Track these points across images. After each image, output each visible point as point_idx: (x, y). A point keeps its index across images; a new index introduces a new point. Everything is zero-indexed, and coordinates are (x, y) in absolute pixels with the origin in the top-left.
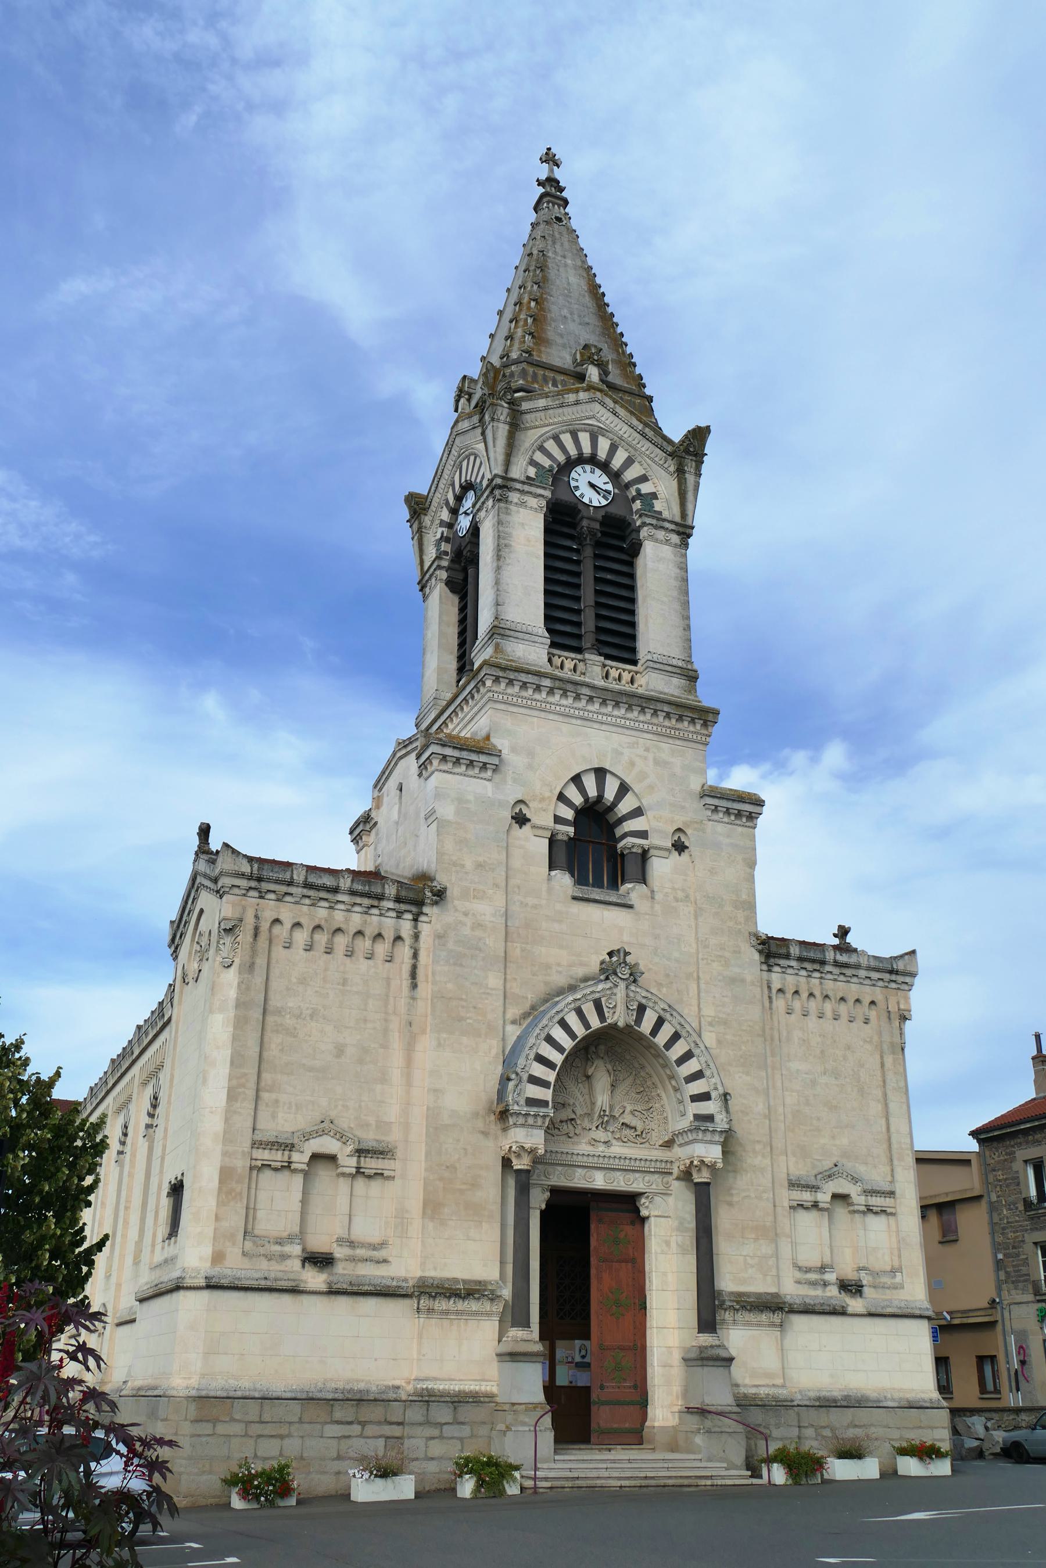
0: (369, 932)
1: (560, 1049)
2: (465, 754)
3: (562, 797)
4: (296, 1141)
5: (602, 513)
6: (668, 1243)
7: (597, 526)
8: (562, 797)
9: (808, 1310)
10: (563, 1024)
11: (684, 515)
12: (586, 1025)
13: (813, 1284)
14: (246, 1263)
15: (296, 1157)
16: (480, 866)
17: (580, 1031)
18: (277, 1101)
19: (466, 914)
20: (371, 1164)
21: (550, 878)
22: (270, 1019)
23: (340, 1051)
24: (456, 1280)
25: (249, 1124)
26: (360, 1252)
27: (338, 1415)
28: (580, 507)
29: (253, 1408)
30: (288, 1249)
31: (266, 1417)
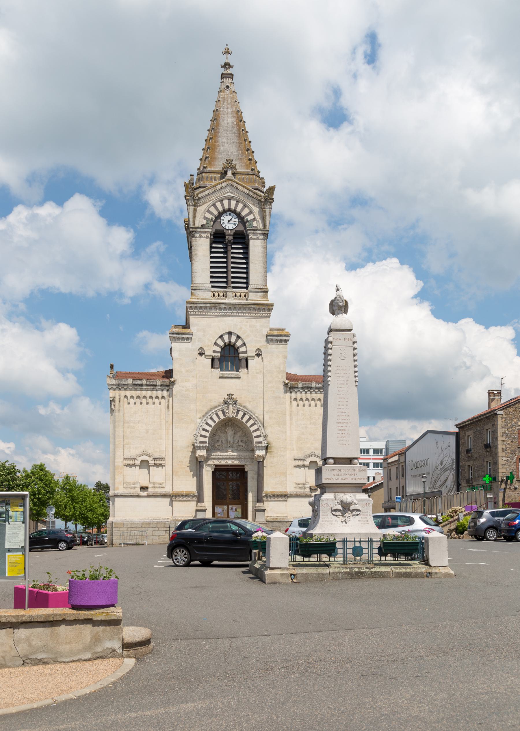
0: (154, 396)
1: (211, 426)
2: (180, 336)
3: (216, 344)
4: (136, 457)
5: (234, 231)
6: (253, 478)
7: (232, 237)
8: (216, 344)
9: (298, 496)
10: (211, 418)
11: (265, 226)
12: (219, 418)
13: (301, 488)
14: (124, 489)
15: (136, 461)
16: (188, 371)
17: (217, 420)
18: (130, 447)
19: (183, 387)
20: (158, 462)
21: (212, 372)
22: (126, 425)
23: (147, 432)
24: (183, 491)
25: (122, 454)
26: (156, 485)
27: (152, 526)
28: (225, 231)
29: (129, 524)
30: (136, 486)
31: (133, 526)
